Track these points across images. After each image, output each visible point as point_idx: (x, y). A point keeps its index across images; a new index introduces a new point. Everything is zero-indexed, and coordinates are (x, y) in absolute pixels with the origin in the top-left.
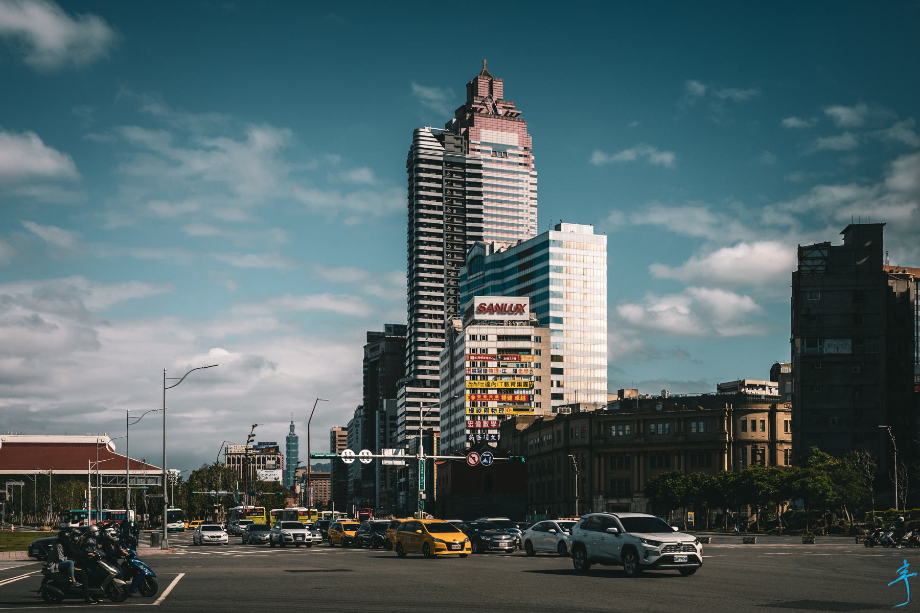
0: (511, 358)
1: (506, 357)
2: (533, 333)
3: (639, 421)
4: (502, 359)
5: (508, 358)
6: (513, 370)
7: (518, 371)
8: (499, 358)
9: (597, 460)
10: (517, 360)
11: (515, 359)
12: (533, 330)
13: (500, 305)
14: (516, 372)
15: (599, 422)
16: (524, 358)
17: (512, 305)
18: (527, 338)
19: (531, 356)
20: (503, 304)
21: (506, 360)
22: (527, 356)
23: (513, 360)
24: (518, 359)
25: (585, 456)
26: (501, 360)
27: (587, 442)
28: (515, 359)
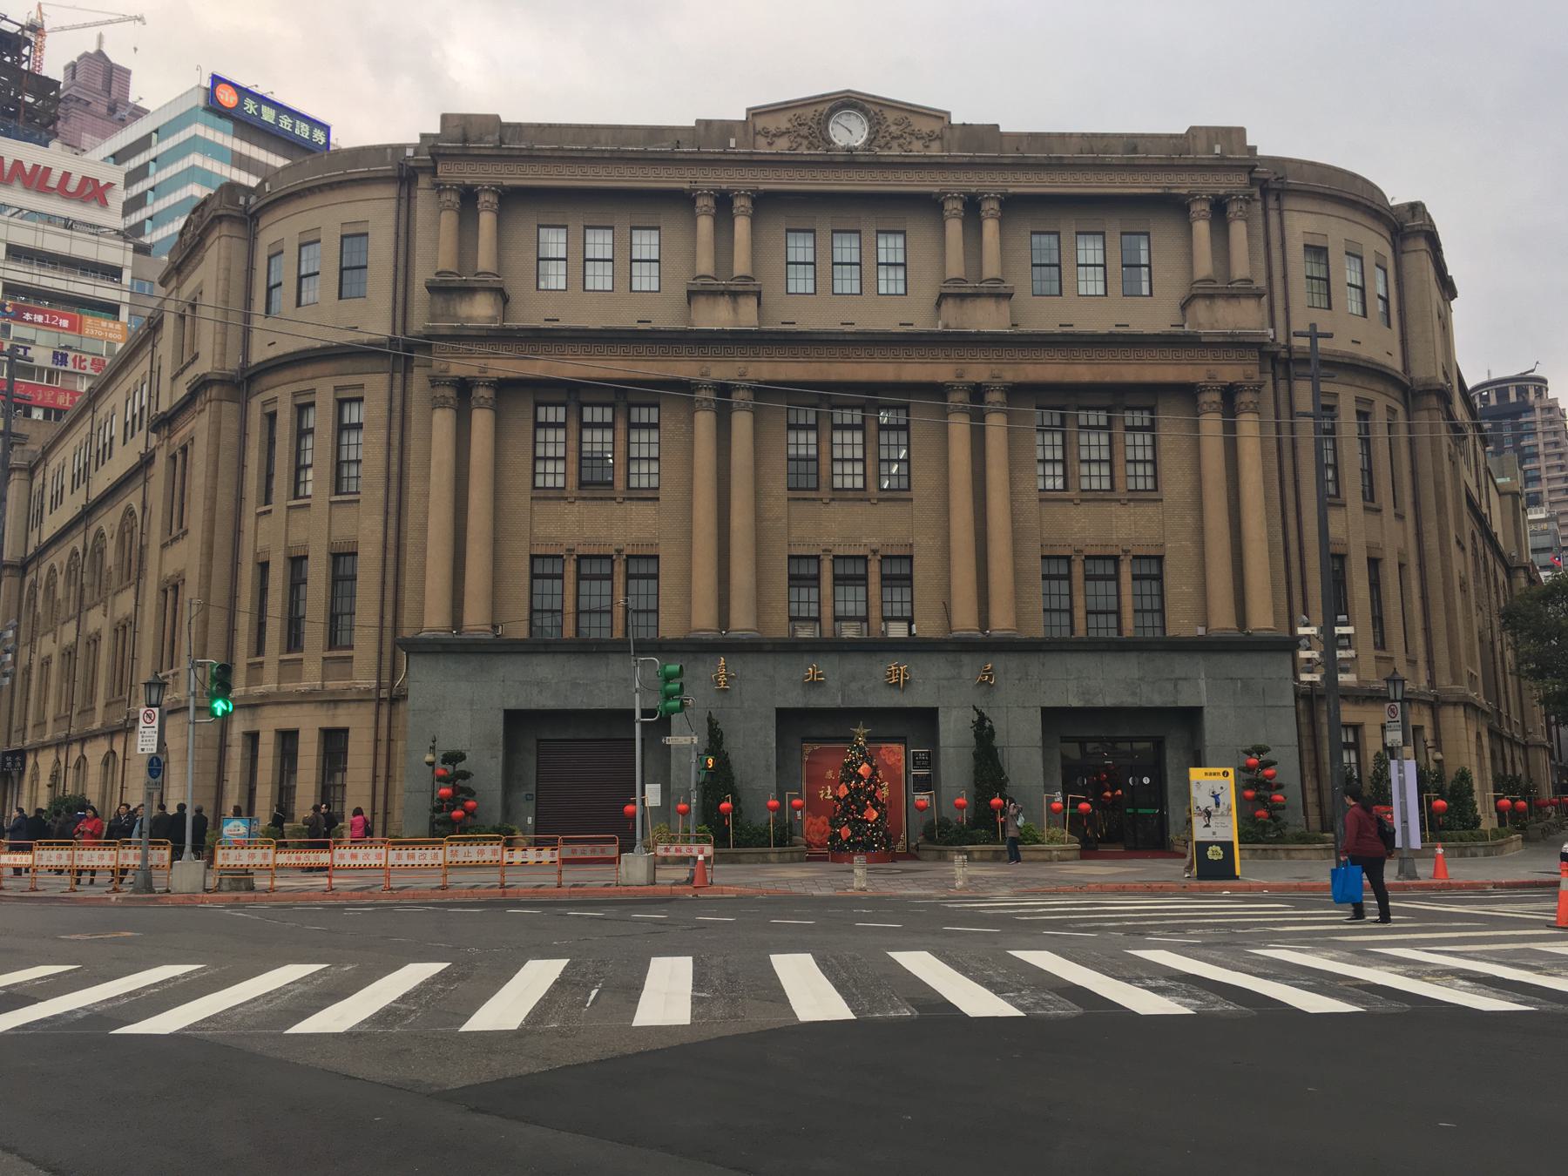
0: (52, 319)
1: (33, 311)
2: (129, 262)
4: (18, 317)
5: (40, 318)
6: (55, 354)
7: (70, 359)
8: (9, 309)
9: (443, 421)
10: (72, 328)
11: (65, 323)
12: (130, 255)
13: (28, 166)
14: (65, 362)
16: (96, 326)
17: (66, 176)
18: (112, 273)
19: (118, 326)
20: (36, 167)
21: (32, 322)
22: (104, 324)
23: (58, 327)
24: (75, 327)
25: (353, 414)
26: (14, 319)
27: (375, 324)
28: (65, 323)
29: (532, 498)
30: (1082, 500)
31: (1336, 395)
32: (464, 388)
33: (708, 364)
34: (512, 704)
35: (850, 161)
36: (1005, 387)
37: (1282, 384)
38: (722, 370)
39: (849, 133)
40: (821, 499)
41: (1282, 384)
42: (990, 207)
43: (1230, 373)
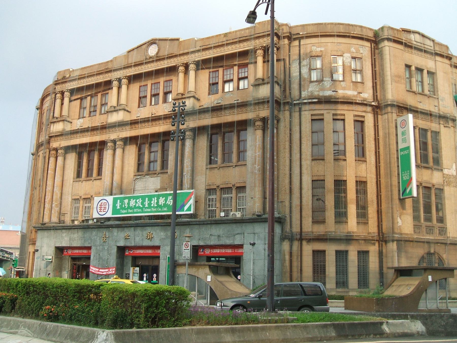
3: (119, 80)
15: (62, 93)
29: (73, 182)
30: (220, 167)
31: (323, 115)
32: (56, 150)
33: (110, 134)
34: (58, 245)
35: (150, 61)
36: (190, 129)
37: (296, 115)
38: (113, 136)
39: (153, 51)
40: (143, 175)
41: (296, 115)
42: (192, 67)
43: (265, 112)
